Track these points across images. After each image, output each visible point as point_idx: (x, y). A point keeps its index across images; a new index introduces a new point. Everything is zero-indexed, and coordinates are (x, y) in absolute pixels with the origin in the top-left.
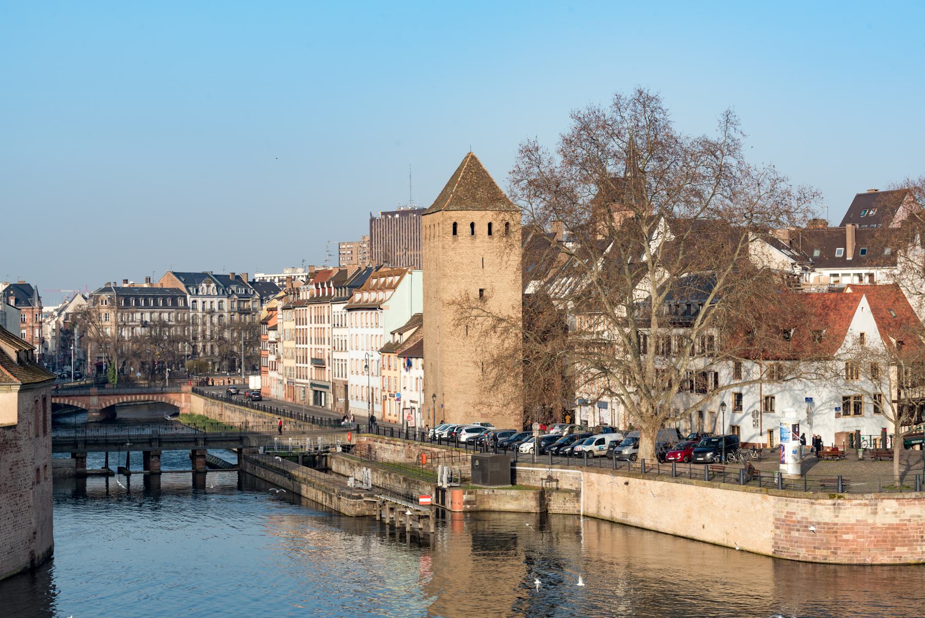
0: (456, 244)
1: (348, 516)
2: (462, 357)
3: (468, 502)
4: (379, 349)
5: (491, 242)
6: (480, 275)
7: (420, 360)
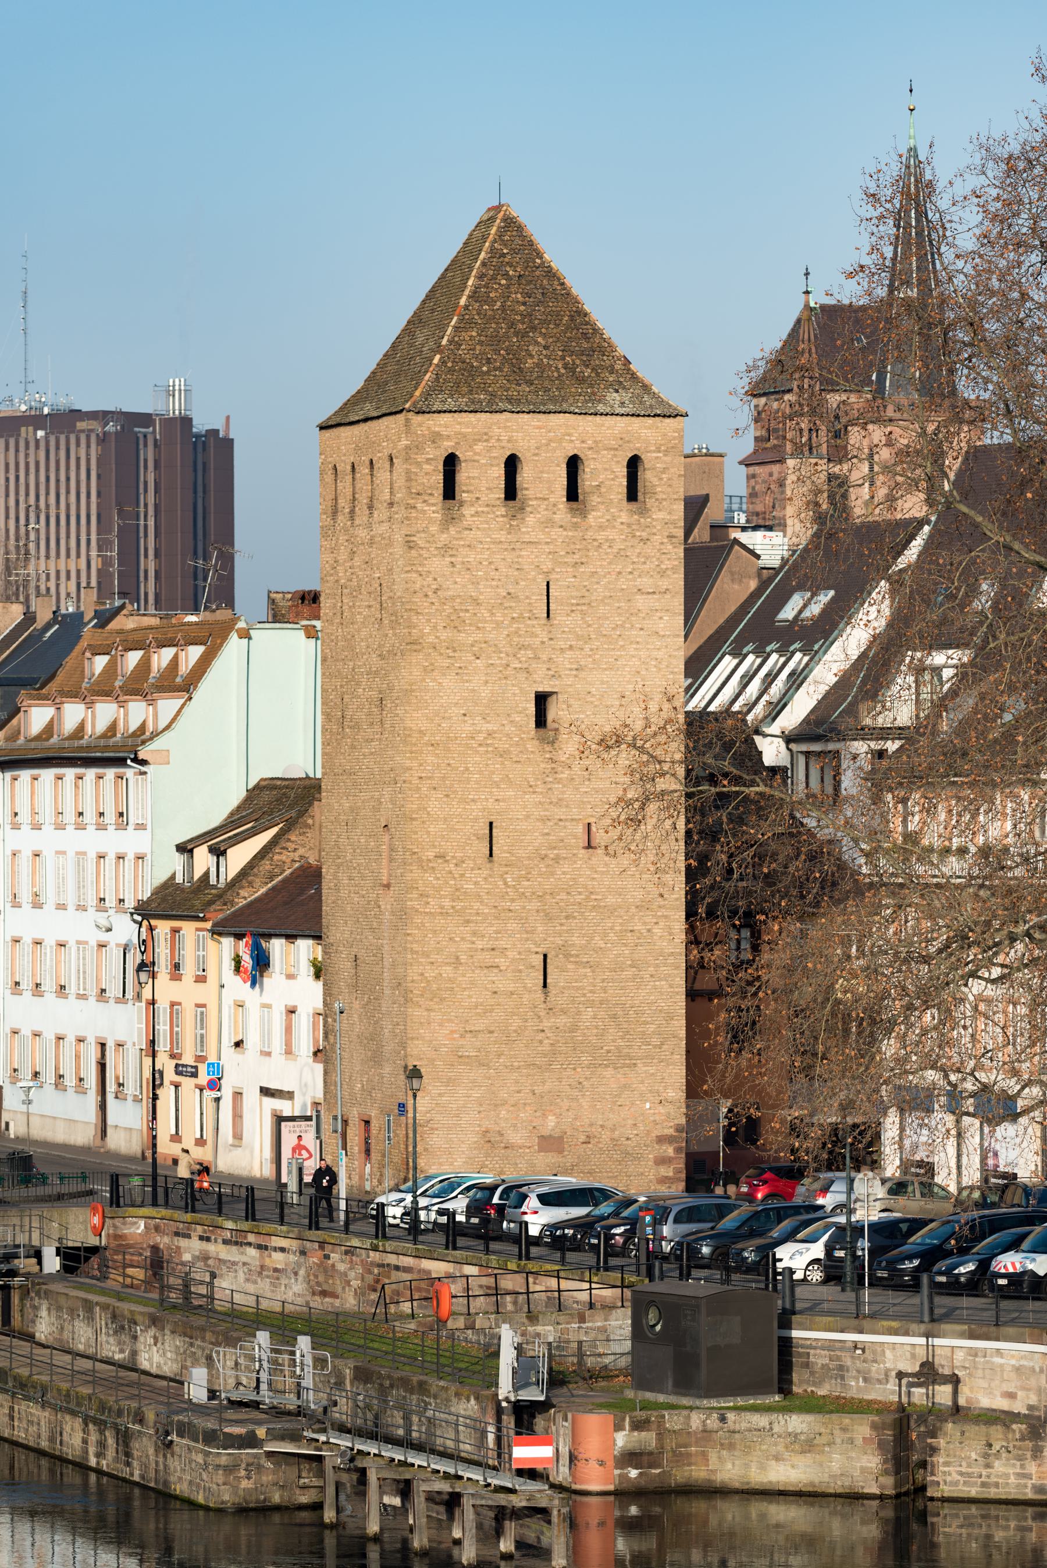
0: (453, 531)
1: (207, 1508)
2: (474, 933)
3: (631, 1457)
4: (130, 904)
5: (575, 526)
6: (537, 641)
7: (305, 948)
